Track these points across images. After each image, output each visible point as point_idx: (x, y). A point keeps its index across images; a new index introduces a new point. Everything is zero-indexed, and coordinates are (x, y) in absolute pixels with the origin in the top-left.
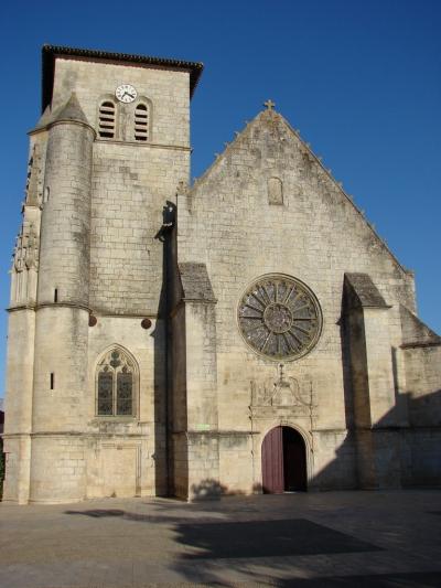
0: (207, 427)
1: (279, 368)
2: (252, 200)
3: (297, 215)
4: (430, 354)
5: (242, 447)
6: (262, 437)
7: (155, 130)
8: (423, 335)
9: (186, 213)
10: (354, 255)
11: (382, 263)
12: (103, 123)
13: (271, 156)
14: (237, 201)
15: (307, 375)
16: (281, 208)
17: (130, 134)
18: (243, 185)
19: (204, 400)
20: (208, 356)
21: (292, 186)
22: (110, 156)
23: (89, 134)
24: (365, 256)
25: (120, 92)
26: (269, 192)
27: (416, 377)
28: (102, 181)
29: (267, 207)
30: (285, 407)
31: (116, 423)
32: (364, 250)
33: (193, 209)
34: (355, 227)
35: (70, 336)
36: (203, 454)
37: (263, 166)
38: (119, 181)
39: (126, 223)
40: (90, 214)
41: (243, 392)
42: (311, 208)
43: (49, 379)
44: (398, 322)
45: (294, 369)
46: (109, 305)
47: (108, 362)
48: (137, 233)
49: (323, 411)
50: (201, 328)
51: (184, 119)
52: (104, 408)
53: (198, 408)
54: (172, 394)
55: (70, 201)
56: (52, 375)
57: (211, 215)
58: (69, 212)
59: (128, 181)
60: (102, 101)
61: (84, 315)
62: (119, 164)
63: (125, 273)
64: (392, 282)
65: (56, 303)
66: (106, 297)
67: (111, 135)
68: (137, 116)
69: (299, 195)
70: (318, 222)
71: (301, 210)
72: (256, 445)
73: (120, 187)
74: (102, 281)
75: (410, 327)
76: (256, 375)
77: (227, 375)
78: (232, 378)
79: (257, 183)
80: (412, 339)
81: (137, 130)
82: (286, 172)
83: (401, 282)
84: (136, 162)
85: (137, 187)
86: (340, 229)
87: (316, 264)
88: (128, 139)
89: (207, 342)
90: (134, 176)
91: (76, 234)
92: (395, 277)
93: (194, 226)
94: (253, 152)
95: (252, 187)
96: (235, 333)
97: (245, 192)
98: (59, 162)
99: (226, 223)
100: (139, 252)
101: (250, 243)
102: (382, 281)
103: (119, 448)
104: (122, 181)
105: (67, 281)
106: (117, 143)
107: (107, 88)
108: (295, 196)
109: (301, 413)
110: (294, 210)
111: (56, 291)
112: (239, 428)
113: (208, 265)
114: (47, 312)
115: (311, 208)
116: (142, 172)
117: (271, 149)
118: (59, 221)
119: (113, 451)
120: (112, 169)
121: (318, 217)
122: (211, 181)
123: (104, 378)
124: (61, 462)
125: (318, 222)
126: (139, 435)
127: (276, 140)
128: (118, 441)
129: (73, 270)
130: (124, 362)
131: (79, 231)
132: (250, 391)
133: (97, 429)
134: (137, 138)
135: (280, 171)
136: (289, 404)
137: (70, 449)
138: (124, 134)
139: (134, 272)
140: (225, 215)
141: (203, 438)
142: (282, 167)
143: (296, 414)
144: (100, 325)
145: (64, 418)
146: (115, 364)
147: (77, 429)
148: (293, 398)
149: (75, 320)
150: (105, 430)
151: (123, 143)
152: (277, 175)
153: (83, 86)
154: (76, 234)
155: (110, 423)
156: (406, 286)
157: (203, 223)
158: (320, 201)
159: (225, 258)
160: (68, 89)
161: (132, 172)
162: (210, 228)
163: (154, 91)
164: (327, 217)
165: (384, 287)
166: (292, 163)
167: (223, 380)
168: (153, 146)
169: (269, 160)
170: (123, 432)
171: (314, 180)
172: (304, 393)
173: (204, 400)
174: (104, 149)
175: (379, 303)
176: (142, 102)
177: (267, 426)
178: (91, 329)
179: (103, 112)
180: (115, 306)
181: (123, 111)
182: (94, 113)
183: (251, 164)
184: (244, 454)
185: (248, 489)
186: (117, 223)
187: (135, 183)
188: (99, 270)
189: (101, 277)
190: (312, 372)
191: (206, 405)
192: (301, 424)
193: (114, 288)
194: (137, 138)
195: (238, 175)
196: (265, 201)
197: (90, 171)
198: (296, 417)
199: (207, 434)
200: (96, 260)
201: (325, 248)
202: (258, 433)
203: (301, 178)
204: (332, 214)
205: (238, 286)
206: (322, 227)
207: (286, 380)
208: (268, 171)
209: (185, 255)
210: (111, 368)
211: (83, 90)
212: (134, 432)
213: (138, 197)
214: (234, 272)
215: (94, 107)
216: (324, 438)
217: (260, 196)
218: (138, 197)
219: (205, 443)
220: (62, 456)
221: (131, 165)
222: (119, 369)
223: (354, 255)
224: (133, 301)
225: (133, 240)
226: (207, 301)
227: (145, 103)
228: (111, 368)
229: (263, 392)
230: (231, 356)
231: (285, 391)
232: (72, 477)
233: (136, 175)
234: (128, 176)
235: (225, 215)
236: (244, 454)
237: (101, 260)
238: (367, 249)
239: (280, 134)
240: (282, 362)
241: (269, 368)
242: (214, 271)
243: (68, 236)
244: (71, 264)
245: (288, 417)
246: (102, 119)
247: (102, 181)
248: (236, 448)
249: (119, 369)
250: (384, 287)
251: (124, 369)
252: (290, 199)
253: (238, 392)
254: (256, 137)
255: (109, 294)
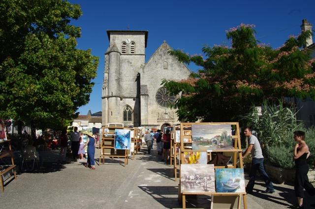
6: (161, 126)
18: (157, 64)
42: (175, 69)
48: (132, 77)
58: (114, 74)
67: (125, 52)
69: (172, 66)
71: (172, 70)
90: (131, 63)
95: (159, 65)
112: (155, 124)
114: (110, 98)
115: (175, 69)
116: (133, 62)
123: (125, 113)
146: (127, 109)
149: (116, 100)
154: (116, 80)
174: (124, 57)
178: (121, 101)
191: (145, 119)
196: (163, 68)
197: (119, 63)
204: (181, 70)
208: (164, 60)
209: (142, 83)
222: (128, 110)
231: (166, 115)
252: (169, 67)
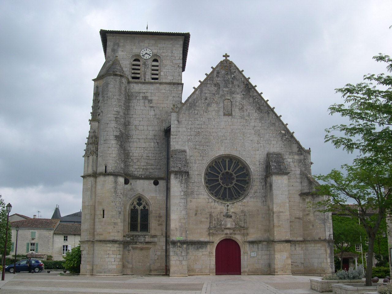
0: (182, 238)
1: (226, 207)
2: (214, 113)
3: (239, 120)
4: (316, 199)
5: (204, 250)
6: (216, 245)
7: (162, 74)
8: (312, 188)
9: (176, 122)
10: (274, 142)
11: (290, 146)
12: (133, 71)
13: (226, 87)
14: (205, 114)
15: (242, 211)
16: (230, 117)
17: (148, 77)
18: (209, 105)
19: (180, 224)
20: (183, 201)
21: (238, 104)
22: (137, 90)
23: (124, 80)
24: (280, 142)
25: (143, 52)
26: (224, 108)
27: (307, 212)
28: (133, 105)
29: (222, 117)
30: (229, 229)
31: (139, 236)
32: (280, 139)
33: (180, 120)
34: (275, 126)
35: (113, 190)
36: (179, 253)
37: (221, 92)
38: (142, 104)
39: (145, 128)
40: (127, 125)
41: (206, 220)
42: (249, 116)
43: (102, 213)
44: (299, 180)
45: (235, 207)
46: (136, 173)
47: (135, 203)
48: (151, 133)
49: (251, 231)
50: (179, 186)
51: (179, 66)
52: (133, 227)
53: (176, 228)
54: (170, 220)
55: (113, 119)
56: (104, 211)
57: (190, 122)
58: (113, 124)
59: (147, 104)
60: (133, 59)
61: (121, 180)
62: (142, 95)
63: (145, 155)
64: (296, 157)
65: (106, 174)
66: (135, 169)
67: (138, 78)
68: (153, 66)
69: (241, 109)
70: (252, 124)
71: (242, 117)
72: (212, 250)
73: (142, 108)
74: (132, 160)
75: (305, 184)
76: (213, 210)
77: (197, 211)
78: (199, 212)
79: (217, 103)
80: (306, 191)
81: (153, 74)
82: (234, 95)
83: (302, 157)
84: (151, 93)
85: (152, 107)
86: (266, 127)
87: (250, 148)
88: (147, 80)
89: (182, 193)
90: (150, 101)
91: (116, 136)
92: (298, 154)
93: (180, 129)
94: (215, 85)
95: (214, 105)
96: (202, 188)
97: (209, 109)
98: (107, 97)
99: (198, 127)
100: (152, 144)
101: (212, 138)
102: (291, 157)
103: (142, 249)
104: (143, 104)
105: (111, 161)
106: (141, 83)
107: (136, 51)
108: (239, 109)
109: (238, 232)
110: (238, 117)
111: (106, 167)
112: (202, 239)
113: (188, 151)
114: (101, 179)
115: (249, 116)
116: (154, 98)
117: (226, 82)
118: (107, 129)
119: (137, 251)
120: (138, 98)
121: (253, 121)
122: (190, 103)
123: (134, 212)
124: (107, 255)
125: (252, 124)
126: (150, 243)
127: (229, 77)
128: (140, 246)
129: (114, 155)
130: (144, 203)
131: (118, 134)
132: (209, 219)
133: (129, 239)
134: (153, 79)
135: (231, 96)
136: (231, 227)
137: (112, 249)
138: (145, 77)
139: (150, 155)
140: (198, 122)
141: (179, 244)
142: (232, 93)
143: (236, 232)
144: (131, 184)
145: (109, 233)
146: (140, 204)
147: (116, 238)
148: (234, 223)
149: (116, 182)
150: (133, 239)
151: (144, 83)
152: (229, 98)
153: (122, 51)
154: (116, 136)
155: (136, 236)
156: (305, 159)
157: (185, 127)
158: (254, 111)
159: (197, 147)
160: (114, 53)
161: (149, 99)
162: (189, 130)
163: (162, 51)
164: (258, 121)
165: (291, 160)
166: (238, 90)
167: (194, 214)
168: (161, 83)
169: (225, 89)
170: (143, 240)
171: (251, 99)
172: (241, 221)
173: (180, 224)
174: (136, 88)
175: (283, 171)
176: (155, 58)
177: (217, 240)
178: (127, 186)
179: (134, 65)
180: (140, 173)
181: (144, 64)
182: (128, 66)
183: (214, 92)
184: (205, 253)
185: (61, 216)
186: (141, 128)
187: (151, 105)
188: (131, 154)
189: (132, 158)
190: (246, 209)
191: (181, 227)
192: (238, 238)
193: (139, 163)
194: (153, 79)
195: (206, 99)
196: (221, 113)
197: (129, 98)
198: (235, 234)
199: (183, 243)
200: (129, 149)
201: (256, 139)
202: (213, 242)
203: (243, 99)
204: (261, 119)
205: (204, 162)
206: (255, 126)
207: (230, 213)
208: (223, 95)
209: (176, 144)
210: (137, 207)
211: (123, 53)
212: (149, 241)
213: (152, 113)
214: (202, 154)
215: (128, 62)
216: (251, 246)
217: (219, 111)
218: (152, 113)
219: (180, 247)
220: (108, 252)
221: (148, 95)
222: (142, 207)
223: (274, 142)
224: (149, 170)
225: (149, 137)
226: (185, 174)
227: (157, 58)
228: (137, 207)
229: (216, 220)
230: (199, 200)
231: (229, 219)
232: (113, 263)
233: (151, 100)
234: (147, 101)
235: (198, 122)
236: (205, 253)
237: (132, 149)
238: (282, 139)
239: (232, 73)
240: (228, 203)
241: (221, 207)
242: (191, 154)
243: (112, 137)
244: (114, 152)
245: (231, 234)
246: (133, 69)
247: (133, 105)
248: (200, 250)
249: (142, 207)
250: (291, 160)
251: (144, 207)
252: (236, 112)
253: (203, 220)
254: (217, 76)
255: (136, 167)
